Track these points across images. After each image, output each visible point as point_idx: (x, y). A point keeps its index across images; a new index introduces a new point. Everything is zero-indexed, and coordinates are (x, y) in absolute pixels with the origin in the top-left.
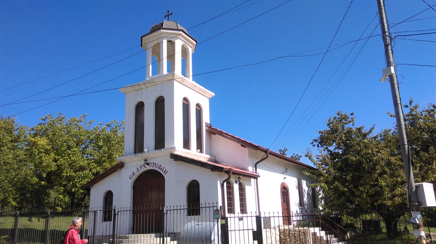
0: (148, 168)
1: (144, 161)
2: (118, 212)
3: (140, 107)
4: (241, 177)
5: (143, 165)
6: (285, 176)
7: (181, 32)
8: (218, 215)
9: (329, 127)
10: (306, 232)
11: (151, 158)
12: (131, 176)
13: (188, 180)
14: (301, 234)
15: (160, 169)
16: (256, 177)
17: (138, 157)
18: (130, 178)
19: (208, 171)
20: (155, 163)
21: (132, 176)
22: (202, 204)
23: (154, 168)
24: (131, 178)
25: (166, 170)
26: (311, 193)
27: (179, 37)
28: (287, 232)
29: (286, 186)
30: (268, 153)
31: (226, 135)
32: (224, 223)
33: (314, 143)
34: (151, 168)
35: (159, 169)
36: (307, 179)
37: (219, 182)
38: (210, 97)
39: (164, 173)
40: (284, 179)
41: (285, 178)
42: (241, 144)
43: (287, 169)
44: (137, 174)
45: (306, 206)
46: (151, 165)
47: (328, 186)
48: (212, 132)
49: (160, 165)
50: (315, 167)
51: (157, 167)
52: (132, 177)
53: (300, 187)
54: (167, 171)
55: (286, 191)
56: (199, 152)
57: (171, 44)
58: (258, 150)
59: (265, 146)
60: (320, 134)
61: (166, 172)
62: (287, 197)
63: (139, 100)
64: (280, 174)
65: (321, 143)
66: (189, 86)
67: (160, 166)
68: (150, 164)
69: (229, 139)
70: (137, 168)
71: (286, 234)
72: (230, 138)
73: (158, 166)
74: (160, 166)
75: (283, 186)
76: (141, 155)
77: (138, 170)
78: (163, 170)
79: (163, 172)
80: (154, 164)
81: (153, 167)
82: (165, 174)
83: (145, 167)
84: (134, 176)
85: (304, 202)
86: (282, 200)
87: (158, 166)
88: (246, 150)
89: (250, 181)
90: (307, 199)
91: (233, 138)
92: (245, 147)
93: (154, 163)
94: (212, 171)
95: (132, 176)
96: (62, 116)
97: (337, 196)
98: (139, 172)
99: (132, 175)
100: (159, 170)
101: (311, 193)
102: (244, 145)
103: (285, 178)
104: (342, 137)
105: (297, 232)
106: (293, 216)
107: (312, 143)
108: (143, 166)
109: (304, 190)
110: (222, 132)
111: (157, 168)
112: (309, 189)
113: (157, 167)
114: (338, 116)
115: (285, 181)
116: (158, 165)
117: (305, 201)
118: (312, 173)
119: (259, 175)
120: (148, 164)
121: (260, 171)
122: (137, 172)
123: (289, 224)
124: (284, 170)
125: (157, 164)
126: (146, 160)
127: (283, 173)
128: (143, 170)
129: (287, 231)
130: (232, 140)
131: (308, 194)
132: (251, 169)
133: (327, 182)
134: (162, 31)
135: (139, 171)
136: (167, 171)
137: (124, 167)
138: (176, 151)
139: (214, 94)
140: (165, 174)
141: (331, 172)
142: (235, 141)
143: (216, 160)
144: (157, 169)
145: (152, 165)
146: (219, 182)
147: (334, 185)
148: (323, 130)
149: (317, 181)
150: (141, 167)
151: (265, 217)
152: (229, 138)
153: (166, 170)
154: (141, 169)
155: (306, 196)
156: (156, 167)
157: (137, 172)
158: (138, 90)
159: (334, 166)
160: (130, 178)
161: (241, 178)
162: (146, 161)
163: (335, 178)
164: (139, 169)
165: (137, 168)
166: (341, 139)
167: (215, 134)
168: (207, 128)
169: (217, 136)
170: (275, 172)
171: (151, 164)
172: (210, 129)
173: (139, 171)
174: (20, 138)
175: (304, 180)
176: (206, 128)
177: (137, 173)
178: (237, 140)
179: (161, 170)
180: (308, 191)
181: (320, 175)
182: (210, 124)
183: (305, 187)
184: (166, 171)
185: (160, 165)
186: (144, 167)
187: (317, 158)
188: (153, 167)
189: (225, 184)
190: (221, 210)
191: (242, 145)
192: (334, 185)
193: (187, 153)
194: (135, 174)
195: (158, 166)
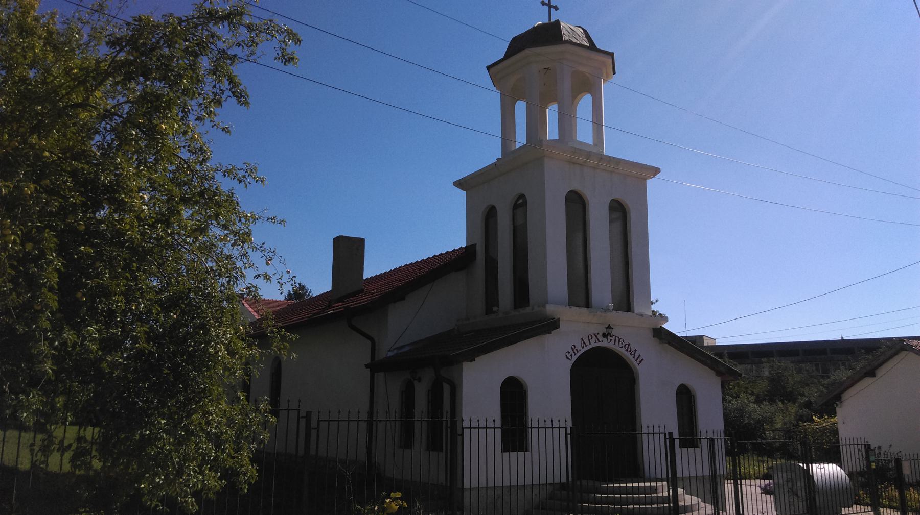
0: (604, 343)
1: (606, 328)
5: (595, 334)
12: (569, 352)
18: (568, 358)
20: (618, 338)
21: (570, 354)
24: (570, 357)
25: (640, 356)
34: (611, 345)
35: (627, 351)
39: (636, 361)
46: (611, 338)
49: (629, 344)
51: (623, 346)
52: (571, 356)
54: (642, 360)
70: (582, 339)
73: (624, 344)
77: (584, 343)
78: (634, 354)
79: (636, 358)
81: (615, 344)
82: (639, 364)
83: (599, 342)
84: (575, 354)
87: (626, 345)
93: (616, 337)
95: (570, 354)
98: (586, 349)
99: (572, 352)
108: (594, 337)
113: (622, 347)
120: (604, 335)
122: (583, 347)
125: (621, 340)
126: (609, 327)
135: (586, 346)
136: (642, 360)
140: (639, 364)
145: (613, 339)
150: (590, 338)
153: (640, 356)
156: (621, 345)
157: (583, 347)
160: (568, 358)
162: (610, 330)
164: (587, 342)
165: (582, 339)
173: (586, 346)
177: (583, 351)
179: (631, 354)
184: (641, 358)
186: (597, 341)
188: (615, 344)
194: (578, 352)
195: (626, 345)
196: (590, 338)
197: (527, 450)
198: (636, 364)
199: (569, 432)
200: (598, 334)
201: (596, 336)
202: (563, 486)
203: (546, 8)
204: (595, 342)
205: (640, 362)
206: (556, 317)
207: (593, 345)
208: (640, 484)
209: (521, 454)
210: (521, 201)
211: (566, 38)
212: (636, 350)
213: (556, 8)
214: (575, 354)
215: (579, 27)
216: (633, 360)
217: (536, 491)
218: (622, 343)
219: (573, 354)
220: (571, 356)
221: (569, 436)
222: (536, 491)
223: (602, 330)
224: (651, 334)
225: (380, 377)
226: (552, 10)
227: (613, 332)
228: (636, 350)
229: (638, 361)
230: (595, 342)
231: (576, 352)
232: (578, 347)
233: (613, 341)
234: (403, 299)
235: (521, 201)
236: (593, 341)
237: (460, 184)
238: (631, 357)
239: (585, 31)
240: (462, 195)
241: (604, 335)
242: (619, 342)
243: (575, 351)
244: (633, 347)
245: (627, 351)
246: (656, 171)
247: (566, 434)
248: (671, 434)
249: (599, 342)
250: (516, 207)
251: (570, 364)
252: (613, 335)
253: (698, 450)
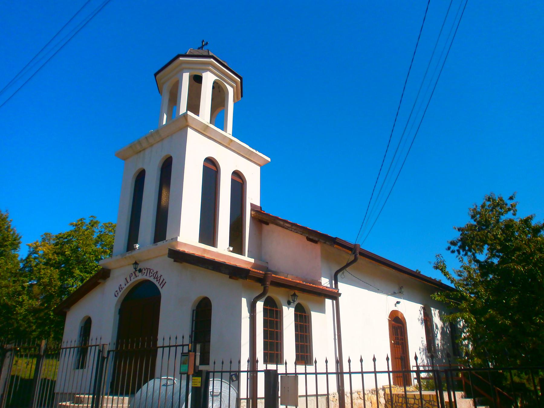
0: (141, 277)
3: (140, 177)
4: (297, 293)
6: (399, 300)
7: (212, 60)
8: (187, 366)
9: (475, 221)
10: (433, 400)
11: (145, 260)
13: (195, 296)
14: (425, 405)
15: (156, 278)
16: (335, 296)
17: (125, 258)
18: (116, 296)
19: (224, 278)
23: (148, 278)
24: (117, 295)
25: (164, 280)
26: (448, 332)
27: (208, 68)
28: (398, 400)
29: (401, 316)
30: (358, 252)
31: (282, 223)
32: (199, 385)
33: (453, 248)
35: (154, 279)
36: (441, 306)
37: (244, 301)
38: (262, 163)
39: (160, 285)
40: (395, 305)
41: (398, 303)
42: (307, 235)
43: (402, 287)
44: (126, 287)
45: (440, 353)
47: (475, 318)
48: (260, 218)
49: (157, 272)
50: (452, 286)
51: (152, 275)
52: (118, 294)
53: (427, 321)
54: (165, 282)
55: (401, 325)
56: (231, 252)
57: (197, 80)
58: (335, 246)
59: (350, 238)
60: (461, 232)
61: (163, 284)
62: (402, 336)
63: (140, 166)
64: (389, 295)
65: (462, 247)
66: (220, 141)
67: (156, 274)
68: (143, 271)
69: (287, 229)
70: (126, 279)
71: (398, 404)
72: (289, 227)
73: (153, 273)
74: (156, 274)
75: (395, 316)
76: (130, 255)
78: (160, 279)
79: (160, 284)
80: (149, 269)
81: (146, 275)
82: (162, 288)
84: (120, 291)
85: (437, 346)
86: (393, 342)
87: (154, 274)
88: (317, 248)
89: (323, 303)
90: (441, 341)
91: (293, 226)
92: (315, 242)
93: (148, 269)
94: (230, 277)
96: (95, 220)
97: (494, 335)
98: (128, 285)
99: (119, 291)
100: (154, 281)
101: (448, 332)
102: (311, 237)
103: (398, 303)
104: (497, 235)
105: (418, 400)
106: (350, 373)
107: (449, 248)
108: (134, 275)
109: (436, 326)
110: (277, 218)
111: (152, 276)
112: (444, 324)
113: (151, 276)
114: (488, 203)
115: (399, 308)
116: (153, 271)
117: (438, 345)
118: (447, 296)
119: (339, 292)
120: (140, 271)
121: (343, 287)
123: (406, 382)
124: (396, 290)
125: (152, 271)
126: (136, 263)
127: (394, 294)
128: (134, 280)
129: (399, 397)
130: (291, 231)
131: (443, 333)
132: (325, 282)
133: (473, 311)
134: (180, 59)
136: (165, 282)
137: (109, 276)
138: (178, 245)
139: (269, 159)
141: (481, 294)
142: (296, 232)
143: (268, 268)
144: (152, 279)
145: (146, 271)
146: (244, 301)
147: (487, 316)
148: (463, 226)
149: (457, 310)
151: (286, 374)
152: (287, 227)
153: (164, 280)
154: (131, 280)
155: (439, 336)
156: (151, 274)
158: (140, 151)
159: (487, 284)
161: (297, 296)
163: (488, 305)
164: (129, 280)
165: (126, 279)
166: (495, 236)
167: (267, 224)
168: (253, 213)
169: (272, 227)
170: (378, 290)
171: (145, 270)
172: (257, 214)
174: (6, 241)
175: (436, 308)
176: (251, 214)
177: (125, 287)
178: (300, 230)
179: (157, 281)
180: (442, 328)
181: (463, 298)
182: (261, 208)
183: (437, 320)
184: (164, 282)
185: (157, 272)
187: (459, 275)
188: (146, 275)
189: (260, 305)
190: (195, 353)
191: (309, 239)
192: (487, 316)
193: (205, 250)
194: (122, 289)
195: (154, 274)
196: (131, 275)
198: (159, 287)
204: (134, 278)
212: (161, 276)
214: (120, 291)
218: (152, 273)
228: (161, 276)
229: (162, 285)
230: (134, 278)
231: (121, 289)
232: (123, 286)
236: (132, 278)
243: (121, 289)
252: (146, 268)
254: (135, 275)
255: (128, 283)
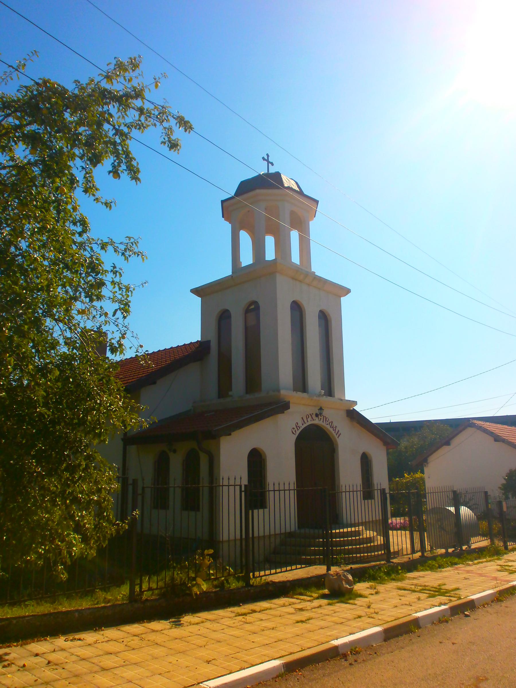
0: (316, 421)
1: (319, 409)
2: (143, 488)
5: (310, 414)
12: (294, 428)
18: (293, 433)
22: (223, 479)
24: (294, 432)
39: (336, 435)
49: (332, 422)
52: (295, 431)
54: (340, 434)
70: (302, 418)
77: (304, 421)
78: (335, 430)
79: (336, 433)
81: (323, 422)
82: (338, 437)
83: (313, 420)
84: (298, 430)
98: (305, 426)
99: (296, 428)
113: (328, 424)
120: (317, 415)
122: (303, 425)
125: (327, 419)
136: (340, 434)
144: (328, 427)
145: (322, 418)
153: (338, 431)
154: (308, 422)
157: (303, 425)
160: (293, 433)
164: (306, 421)
165: (302, 418)
173: (305, 423)
179: (333, 430)
184: (339, 433)
186: (312, 420)
188: (323, 422)
197: (266, 507)
198: (336, 437)
199: (243, 489)
200: (313, 414)
201: (311, 416)
202: (290, 535)
203: (266, 163)
205: (339, 436)
206: (287, 400)
207: (310, 423)
208: (354, 530)
209: (261, 511)
210: (253, 307)
211: (286, 185)
213: (272, 164)
215: (292, 179)
216: (335, 435)
217: (272, 539)
219: (297, 430)
220: (295, 431)
221: (243, 494)
222: (272, 539)
223: (316, 411)
224: (344, 414)
225: (132, 449)
226: (270, 165)
227: (325, 413)
229: (338, 435)
231: (298, 427)
232: (300, 424)
233: (322, 420)
234: (155, 383)
235: (253, 307)
236: (309, 419)
237: (196, 291)
238: (333, 432)
239: (297, 183)
240: (197, 301)
241: (317, 415)
242: (326, 420)
243: (298, 427)
244: (335, 424)
245: (331, 427)
246: (347, 291)
247: (241, 491)
248: (384, 490)
249: (313, 420)
250: (247, 311)
251: (295, 437)
253: (373, 501)
254: (312, 417)
255: (305, 423)
